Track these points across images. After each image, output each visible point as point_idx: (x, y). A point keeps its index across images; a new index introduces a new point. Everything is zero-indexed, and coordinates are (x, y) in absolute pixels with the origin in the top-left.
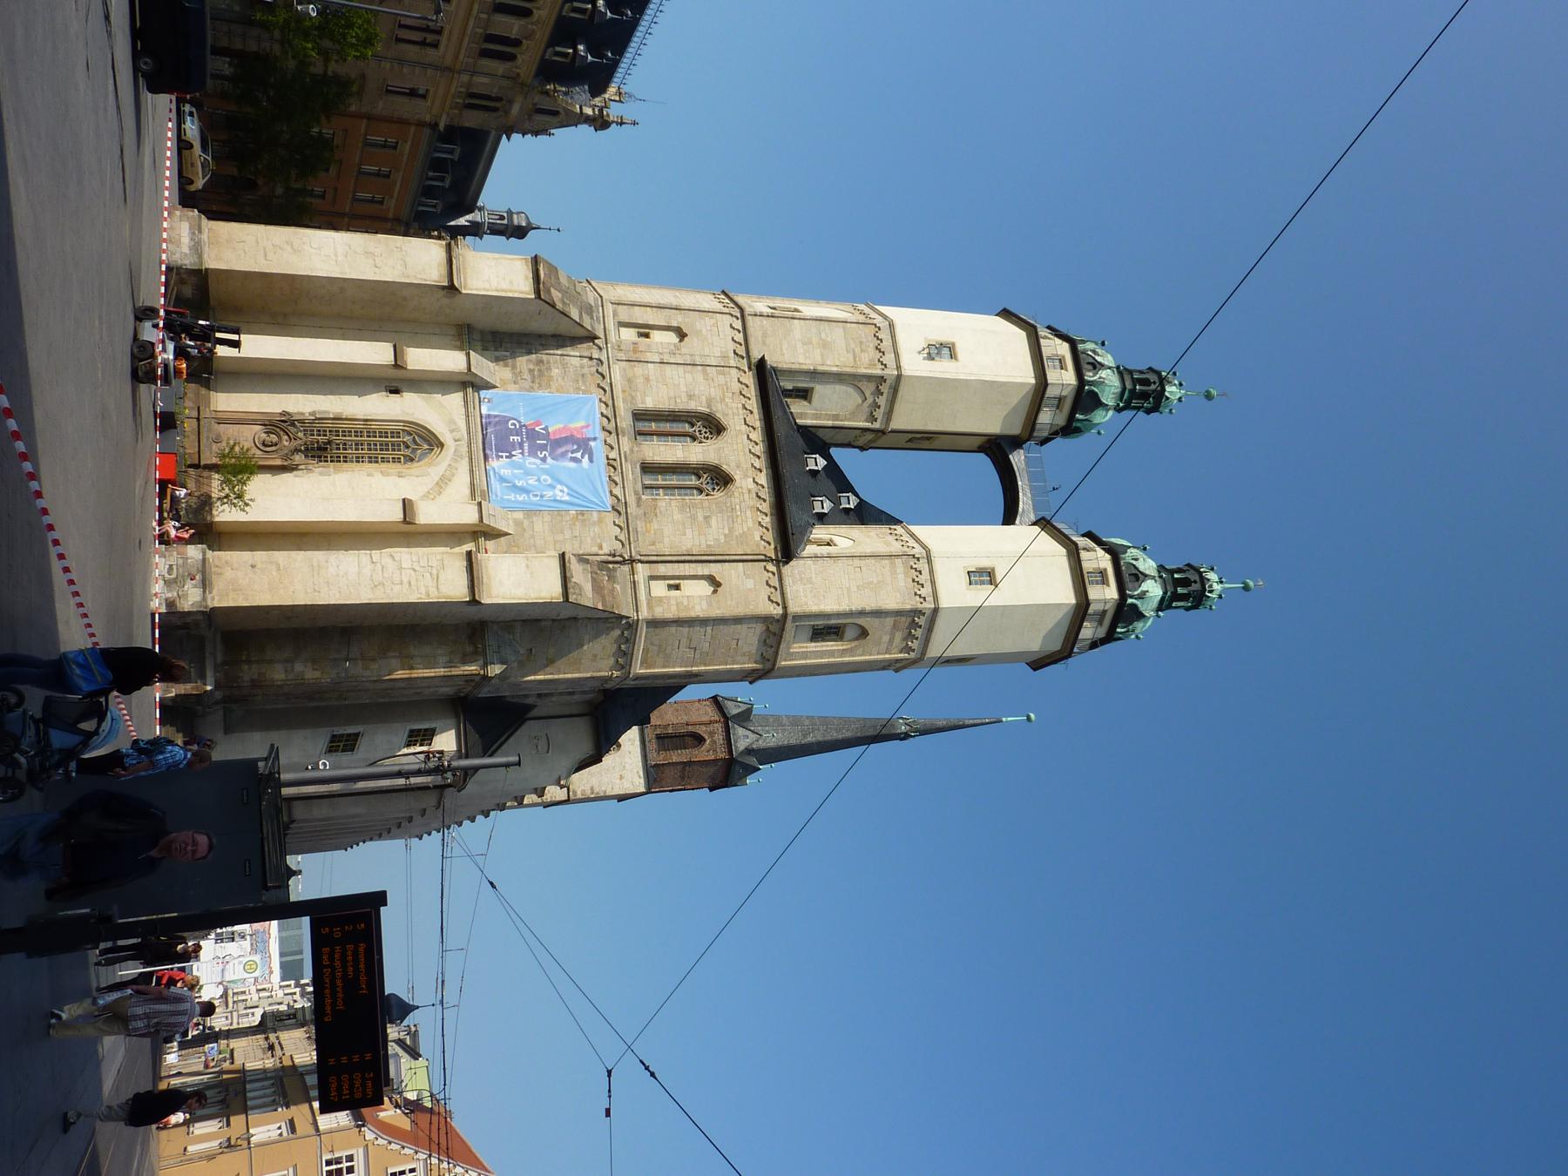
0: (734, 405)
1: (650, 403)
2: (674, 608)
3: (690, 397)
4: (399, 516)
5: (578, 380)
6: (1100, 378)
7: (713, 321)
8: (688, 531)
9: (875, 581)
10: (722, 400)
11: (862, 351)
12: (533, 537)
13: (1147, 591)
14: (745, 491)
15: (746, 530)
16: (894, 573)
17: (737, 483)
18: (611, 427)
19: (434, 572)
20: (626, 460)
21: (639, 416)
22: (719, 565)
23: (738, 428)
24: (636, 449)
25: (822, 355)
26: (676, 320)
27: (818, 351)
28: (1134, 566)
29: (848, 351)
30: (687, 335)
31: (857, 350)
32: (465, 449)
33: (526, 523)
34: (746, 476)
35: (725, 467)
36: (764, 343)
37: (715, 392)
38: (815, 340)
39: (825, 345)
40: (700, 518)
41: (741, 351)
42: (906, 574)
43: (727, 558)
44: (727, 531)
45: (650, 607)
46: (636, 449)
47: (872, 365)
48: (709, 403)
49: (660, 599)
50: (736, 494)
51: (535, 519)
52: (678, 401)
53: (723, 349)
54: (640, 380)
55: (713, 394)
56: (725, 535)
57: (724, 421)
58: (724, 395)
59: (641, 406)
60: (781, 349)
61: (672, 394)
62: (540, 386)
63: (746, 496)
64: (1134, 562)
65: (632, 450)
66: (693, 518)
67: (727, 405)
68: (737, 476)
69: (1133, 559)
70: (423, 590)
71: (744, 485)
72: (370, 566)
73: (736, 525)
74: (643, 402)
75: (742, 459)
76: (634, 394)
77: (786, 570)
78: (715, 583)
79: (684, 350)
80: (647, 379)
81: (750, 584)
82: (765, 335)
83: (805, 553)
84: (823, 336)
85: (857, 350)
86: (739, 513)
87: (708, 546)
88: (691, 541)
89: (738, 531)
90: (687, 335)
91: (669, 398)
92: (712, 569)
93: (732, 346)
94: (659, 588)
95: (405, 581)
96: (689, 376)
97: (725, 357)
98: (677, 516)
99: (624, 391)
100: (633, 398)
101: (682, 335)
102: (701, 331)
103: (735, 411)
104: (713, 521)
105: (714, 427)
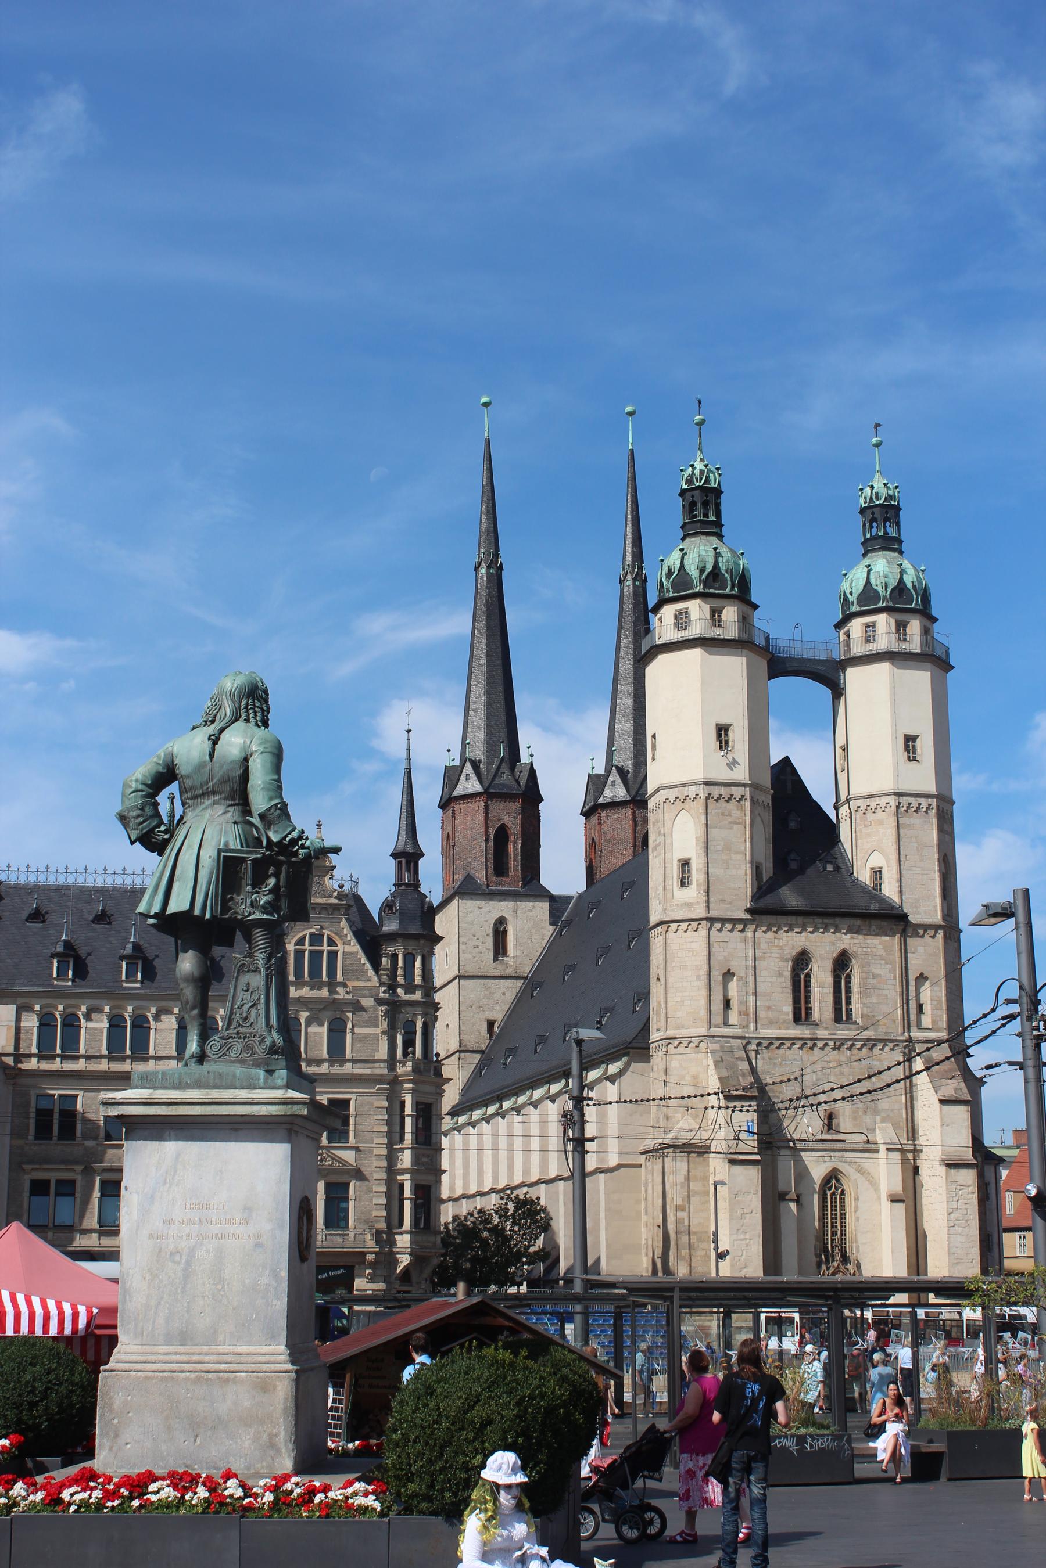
0: (785, 939)
1: (788, 1009)
2: (939, 1012)
3: (780, 975)
4: (901, 1206)
5: (775, 1064)
6: (727, 572)
7: (715, 944)
8: (885, 992)
9: (916, 844)
10: (781, 948)
11: (730, 815)
12: (892, 1110)
13: (913, 582)
14: (852, 941)
15: (881, 946)
16: (910, 827)
17: (847, 947)
18: (810, 1044)
19: (958, 1187)
20: (835, 1034)
21: (797, 1019)
22: (910, 972)
23: (803, 939)
24: (824, 1025)
25: (737, 853)
26: (717, 976)
27: (733, 856)
28: (893, 590)
29: (731, 828)
30: (729, 970)
31: (730, 819)
32: (837, 1154)
33: (883, 1114)
34: (841, 939)
35: (835, 955)
36: (730, 903)
37: (776, 953)
38: (724, 857)
39: (728, 848)
40: (874, 981)
41: (740, 927)
42: (911, 817)
43: (904, 965)
44: (883, 962)
45: (938, 1030)
46: (824, 1025)
47: (742, 809)
48: (787, 960)
49: (933, 1022)
50: (855, 949)
51: (880, 1107)
52: (784, 985)
53: (739, 940)
54: (770, 1014)
55: (777, 955)
56: (886, 963)
57: (798, 950)
58: (777, 946)
59: (791, 1016)
60: (734, 889)
61: (779, 990)
62: (780, 1092)
63: (856, 941)
64: (889, 590)
65: (826, 1029)
66: (874, 987)
67: (785, 945)
68: (841, 946)
69: (886, 589)
70: (970, 1196)
71: (848, 941)
72: (956, 1228)
73: (878, 954)
74: (787, 1014)
75: (827, 940)
76: (781, 1021)
77: (913, 919)
78: (922, 978)
79: (743, 974)
80: (769, 1008)
81: (921, 950)
82: (723, 901)
83: (896, 899)
84: (719, 848)
85: (730, 819)
86: (869, 950)
87: (895, 978)
88: (892, 990)
89: (881, 952)
90: (729, 970)
91: (783, 992)
92: (912, 976)
93: (736, 933)
94: (926, 1021)
95: (965, 1206)
96: (764, 973)
97: (745, 940)
98: (874, 1000)
99: (780, 1028)
100: (784, 1021)
101: (728, 975)
102: (725, 957)
103: (789, 939)
104: (877, 971)
105: (801, 961)
